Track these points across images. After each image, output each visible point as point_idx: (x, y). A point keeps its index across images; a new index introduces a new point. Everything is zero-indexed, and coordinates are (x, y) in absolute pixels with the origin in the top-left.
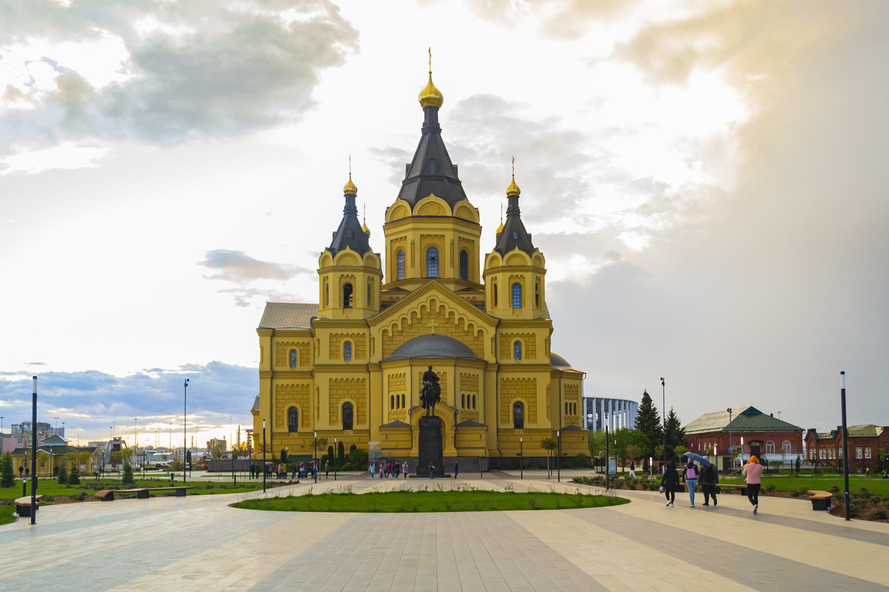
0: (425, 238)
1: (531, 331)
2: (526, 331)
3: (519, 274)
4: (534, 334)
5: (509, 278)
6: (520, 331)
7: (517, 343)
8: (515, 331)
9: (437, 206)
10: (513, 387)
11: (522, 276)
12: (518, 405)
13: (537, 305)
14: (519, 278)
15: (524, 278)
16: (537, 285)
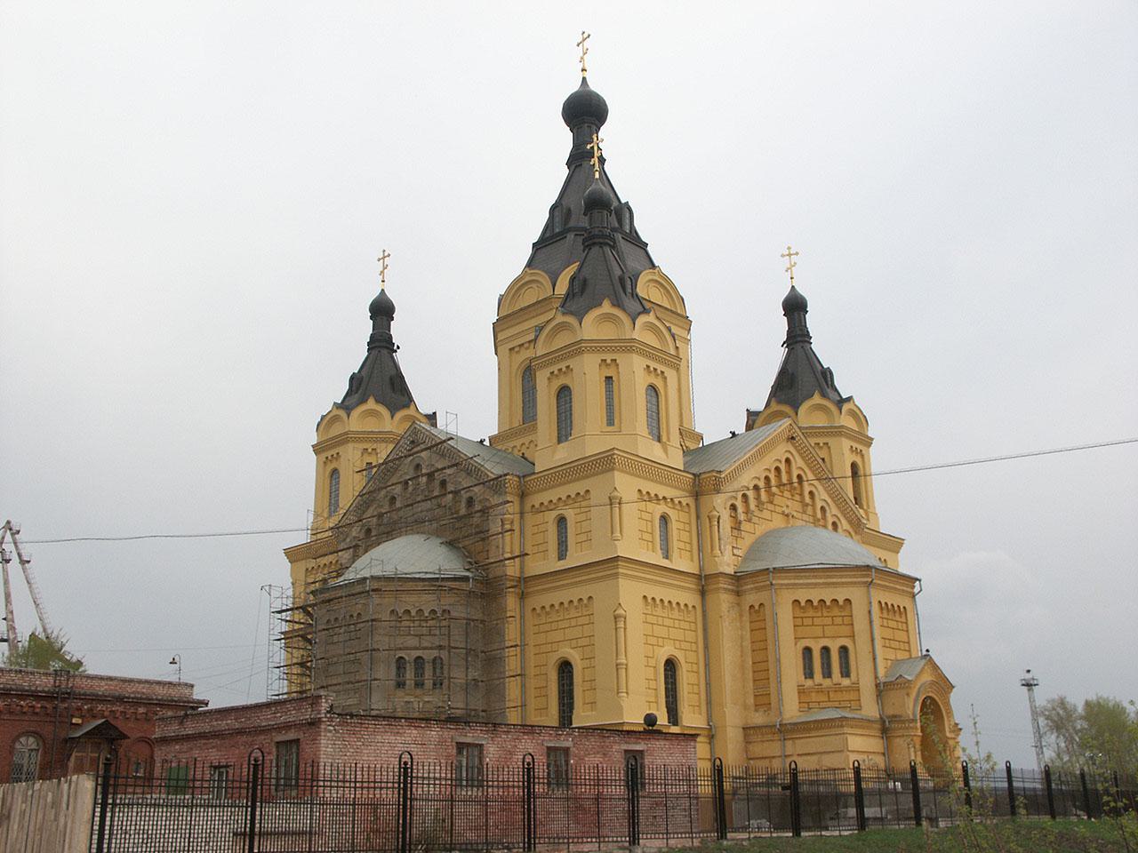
0: (517, 352)
1: (579, 487)
2: (572, 489)
3: (563, 366)
4: (588, 491)
5: (549, 379)
6: (562, 492)
7: (562, 521)
8: (553, 495)
9: (534, 285)
10: (554, 626)
11: (568, 367)
12: (565, 668)
13: (610, 422)
14: (565, 373)
15: (572, 370)
16: (609, 379)
